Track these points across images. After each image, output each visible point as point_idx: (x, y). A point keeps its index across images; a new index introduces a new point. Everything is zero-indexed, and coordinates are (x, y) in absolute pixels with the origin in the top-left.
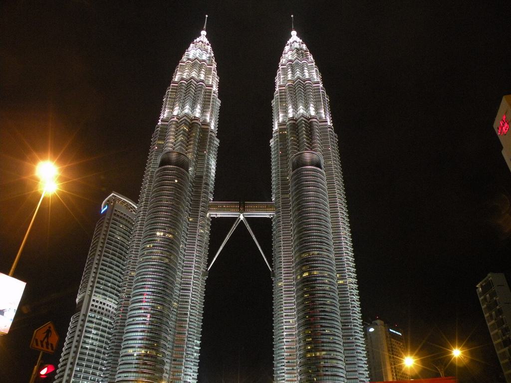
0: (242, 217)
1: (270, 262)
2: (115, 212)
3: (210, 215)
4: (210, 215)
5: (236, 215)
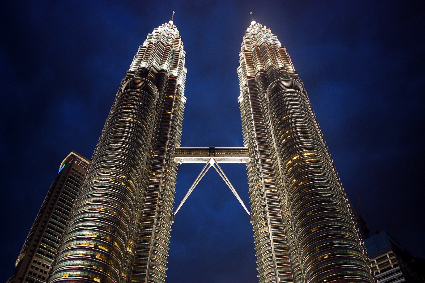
0: (212, 163)
1: (248, 206)
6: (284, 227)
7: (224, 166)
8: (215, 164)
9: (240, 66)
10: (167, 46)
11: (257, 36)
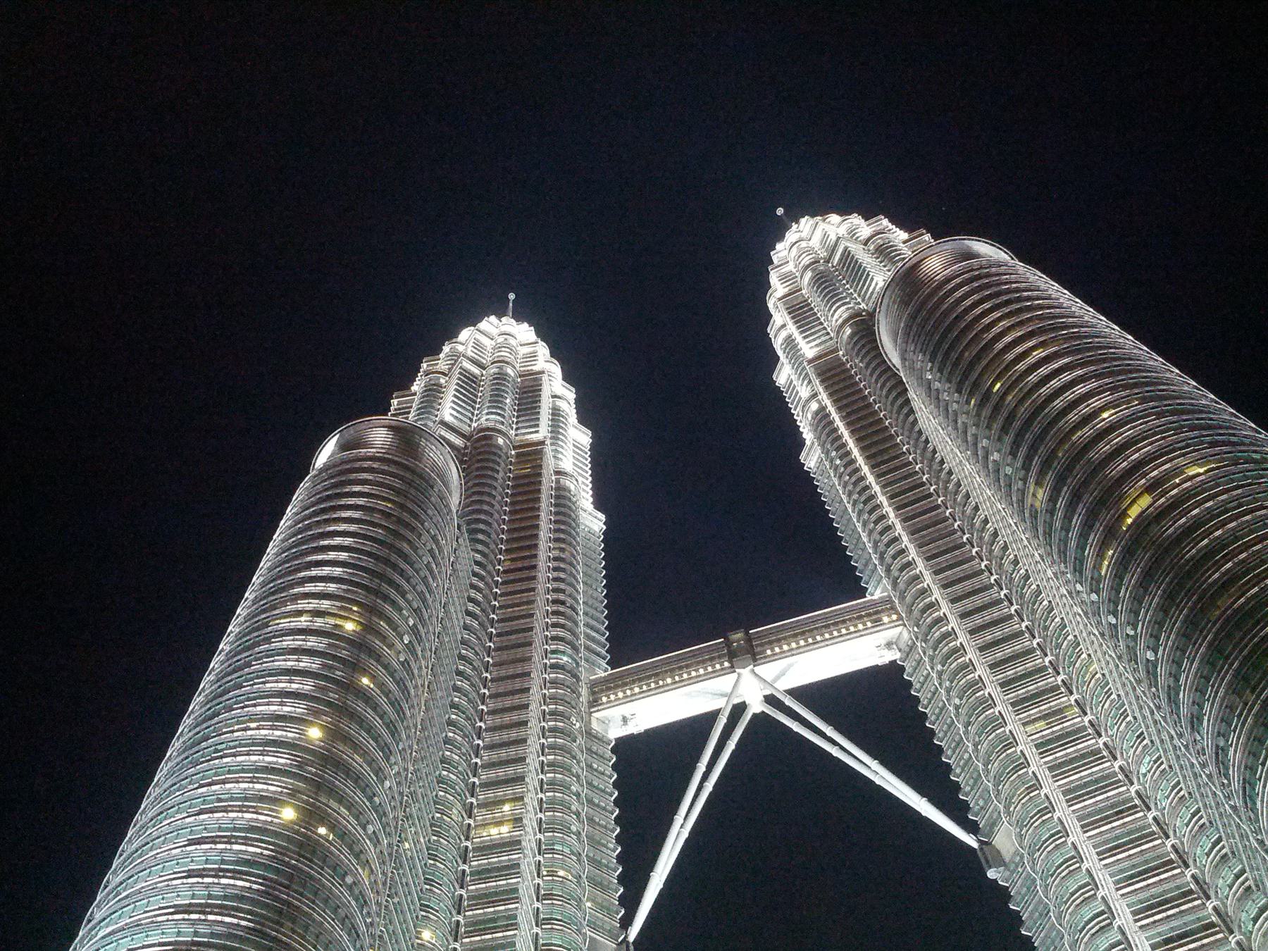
1: (958, 811)
3: (601, 721)
9: (781, 358)
11: (811, 243)
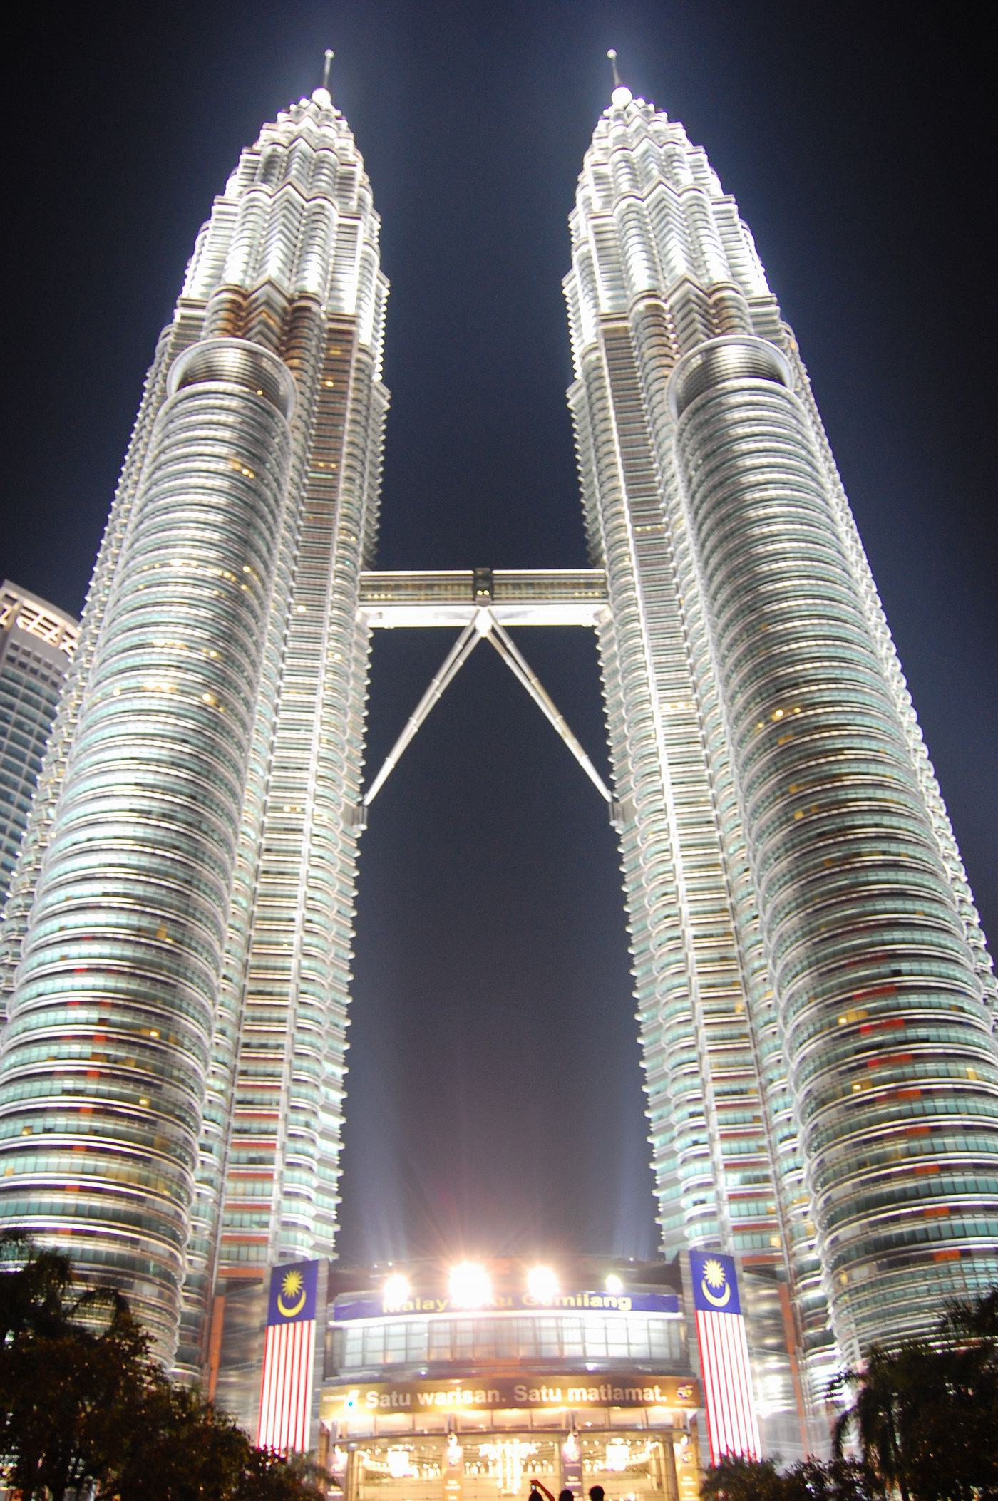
1: (604, 769)
2: (12, 653)
3: (365, 616)
4: (365, 616)
5: (461, 617)
6: (721, 844)
7: (523, 636)
8: (493, 631)
10: (314, 199)
